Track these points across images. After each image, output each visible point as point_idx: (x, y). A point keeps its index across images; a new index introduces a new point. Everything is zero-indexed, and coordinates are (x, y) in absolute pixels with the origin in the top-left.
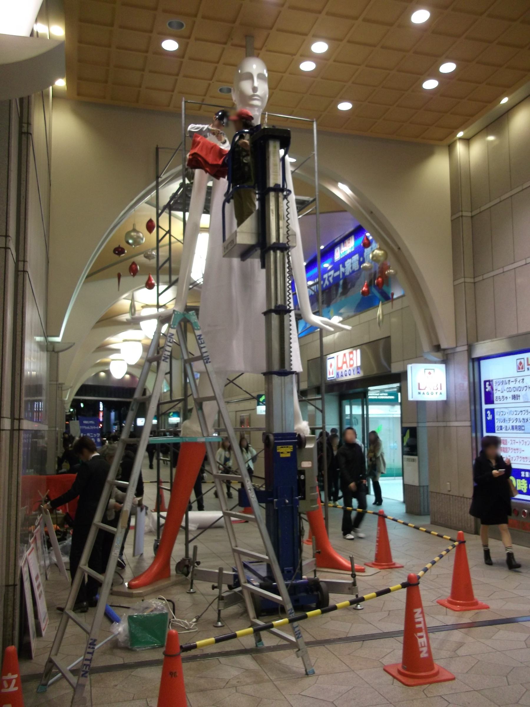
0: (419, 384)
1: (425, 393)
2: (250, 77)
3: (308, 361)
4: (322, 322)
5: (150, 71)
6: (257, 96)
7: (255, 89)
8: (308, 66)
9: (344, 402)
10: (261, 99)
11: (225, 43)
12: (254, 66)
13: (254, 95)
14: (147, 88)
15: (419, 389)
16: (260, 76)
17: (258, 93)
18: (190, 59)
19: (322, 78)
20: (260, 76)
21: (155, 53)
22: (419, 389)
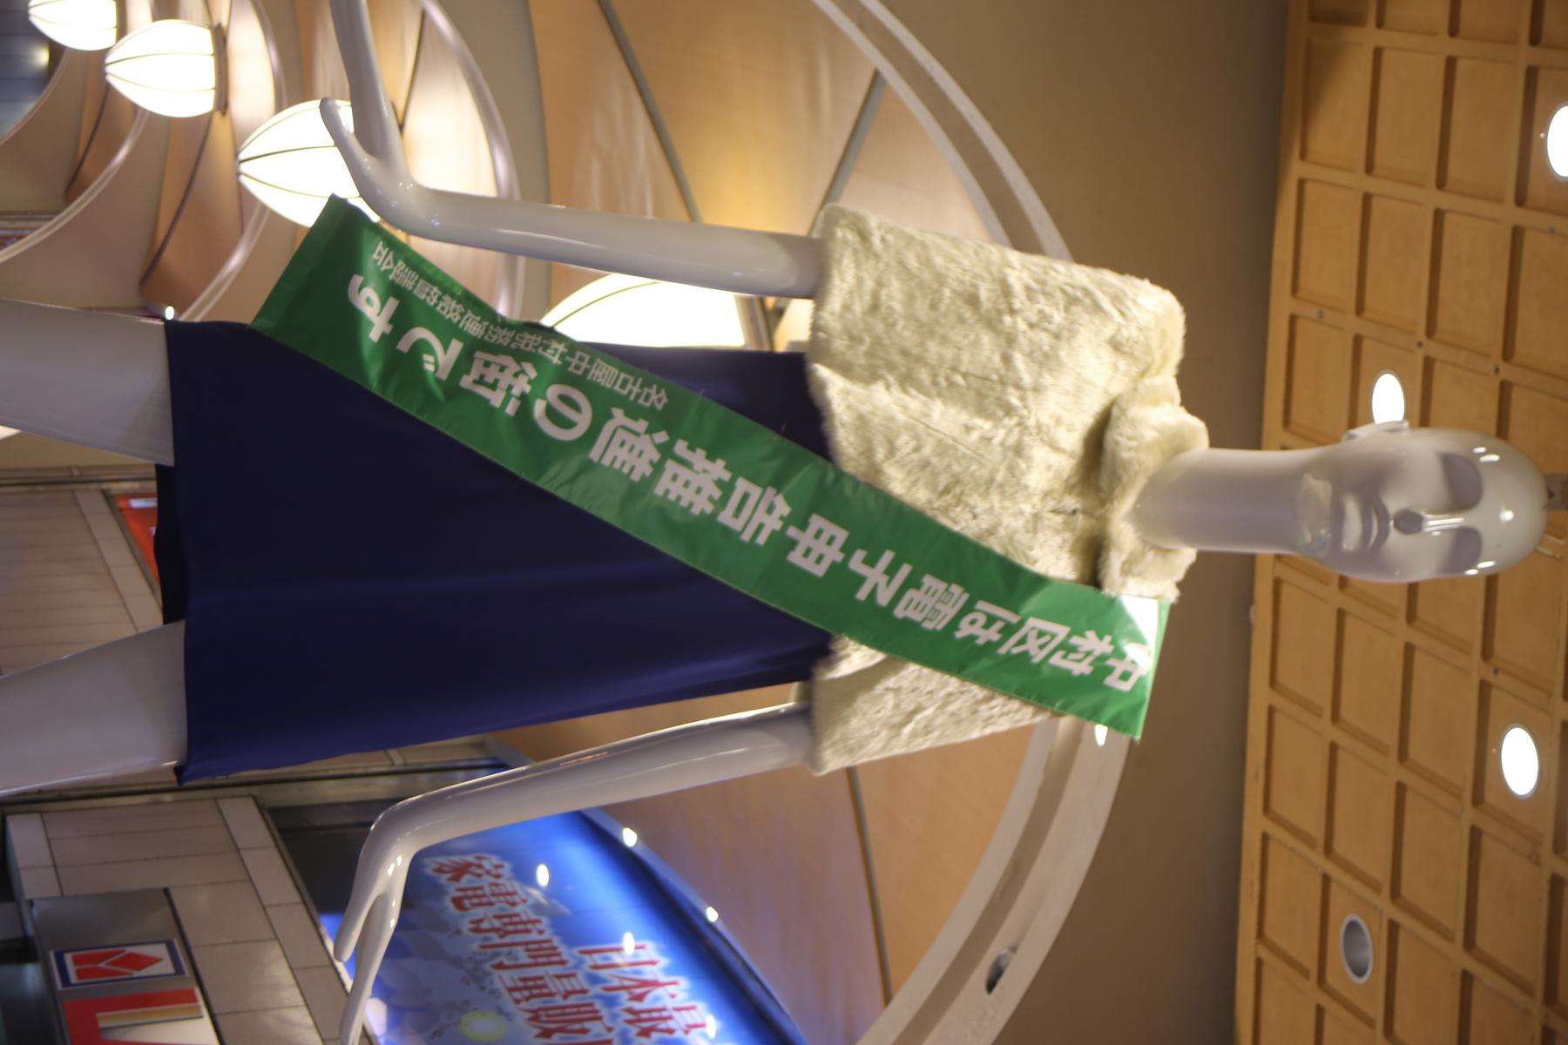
3: (166, 891)
4: (383, 900)
5: (1451, 64)
6: (1383, 533)
7: (1410, 522)
10: (1371, 553)
12: (1508, 515)
13: (1383, 516)
14: (1378, 53)
17: (1394, 536)
18: (1517, 234)
20: (1465, 544)
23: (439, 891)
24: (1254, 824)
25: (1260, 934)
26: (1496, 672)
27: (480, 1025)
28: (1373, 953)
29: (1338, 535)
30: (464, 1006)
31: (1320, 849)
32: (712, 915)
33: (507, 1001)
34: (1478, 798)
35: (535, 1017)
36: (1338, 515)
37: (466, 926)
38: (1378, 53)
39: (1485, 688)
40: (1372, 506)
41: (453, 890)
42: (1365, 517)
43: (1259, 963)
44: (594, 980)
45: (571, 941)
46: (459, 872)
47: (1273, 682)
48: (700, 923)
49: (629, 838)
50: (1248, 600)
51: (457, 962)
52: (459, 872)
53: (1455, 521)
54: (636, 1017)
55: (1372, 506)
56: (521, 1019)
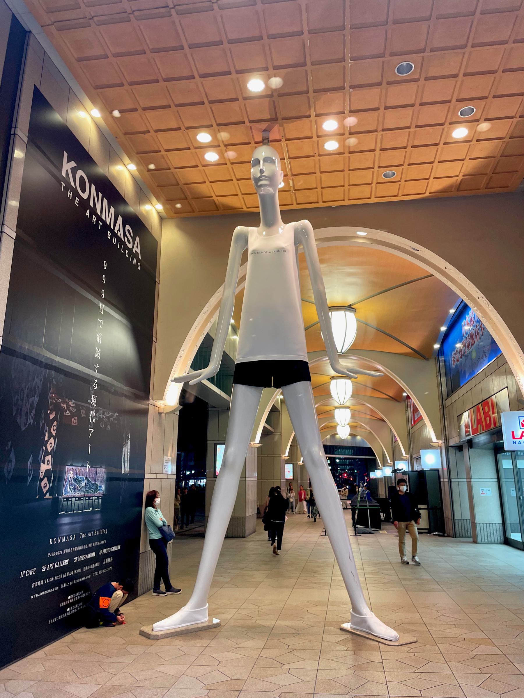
0: (513, 433)
1: (522, 442)
2: (257, 162)
6: (264, 176)
7: (262, 171)
8: (331, 146)
9: (500, 456)
11: (249, 143)
12: (263, 154)
13: (261, 177)
14: (217, 196)
15: (514, 438)
16: (266, 160)
18: (232, 163)
21: (204, 166)
22: (514, 438)
23: (457, 364)
24: (373, 200)
27: (474, 355)
28: (389, 171)
29: (266, 185)
30: (471, 359)
32: (452, 311)
33: (471, 350)
35: (472, 344)
36: (261, 186)
37: (461, 359)
38: (217, 196)
39: (320, 155)
41: (456, 362)
42: (261, 180)
44: (467, 333)
45: (462, 339)
46: (454, 361)
47: (343, 200)
48: (457, 313)
49: (443, 329)
50: (331, 207)
51: (466, 360)
52: (454, 361)
53: (261, 162)
54: (472, 325)
56: (473, 347)
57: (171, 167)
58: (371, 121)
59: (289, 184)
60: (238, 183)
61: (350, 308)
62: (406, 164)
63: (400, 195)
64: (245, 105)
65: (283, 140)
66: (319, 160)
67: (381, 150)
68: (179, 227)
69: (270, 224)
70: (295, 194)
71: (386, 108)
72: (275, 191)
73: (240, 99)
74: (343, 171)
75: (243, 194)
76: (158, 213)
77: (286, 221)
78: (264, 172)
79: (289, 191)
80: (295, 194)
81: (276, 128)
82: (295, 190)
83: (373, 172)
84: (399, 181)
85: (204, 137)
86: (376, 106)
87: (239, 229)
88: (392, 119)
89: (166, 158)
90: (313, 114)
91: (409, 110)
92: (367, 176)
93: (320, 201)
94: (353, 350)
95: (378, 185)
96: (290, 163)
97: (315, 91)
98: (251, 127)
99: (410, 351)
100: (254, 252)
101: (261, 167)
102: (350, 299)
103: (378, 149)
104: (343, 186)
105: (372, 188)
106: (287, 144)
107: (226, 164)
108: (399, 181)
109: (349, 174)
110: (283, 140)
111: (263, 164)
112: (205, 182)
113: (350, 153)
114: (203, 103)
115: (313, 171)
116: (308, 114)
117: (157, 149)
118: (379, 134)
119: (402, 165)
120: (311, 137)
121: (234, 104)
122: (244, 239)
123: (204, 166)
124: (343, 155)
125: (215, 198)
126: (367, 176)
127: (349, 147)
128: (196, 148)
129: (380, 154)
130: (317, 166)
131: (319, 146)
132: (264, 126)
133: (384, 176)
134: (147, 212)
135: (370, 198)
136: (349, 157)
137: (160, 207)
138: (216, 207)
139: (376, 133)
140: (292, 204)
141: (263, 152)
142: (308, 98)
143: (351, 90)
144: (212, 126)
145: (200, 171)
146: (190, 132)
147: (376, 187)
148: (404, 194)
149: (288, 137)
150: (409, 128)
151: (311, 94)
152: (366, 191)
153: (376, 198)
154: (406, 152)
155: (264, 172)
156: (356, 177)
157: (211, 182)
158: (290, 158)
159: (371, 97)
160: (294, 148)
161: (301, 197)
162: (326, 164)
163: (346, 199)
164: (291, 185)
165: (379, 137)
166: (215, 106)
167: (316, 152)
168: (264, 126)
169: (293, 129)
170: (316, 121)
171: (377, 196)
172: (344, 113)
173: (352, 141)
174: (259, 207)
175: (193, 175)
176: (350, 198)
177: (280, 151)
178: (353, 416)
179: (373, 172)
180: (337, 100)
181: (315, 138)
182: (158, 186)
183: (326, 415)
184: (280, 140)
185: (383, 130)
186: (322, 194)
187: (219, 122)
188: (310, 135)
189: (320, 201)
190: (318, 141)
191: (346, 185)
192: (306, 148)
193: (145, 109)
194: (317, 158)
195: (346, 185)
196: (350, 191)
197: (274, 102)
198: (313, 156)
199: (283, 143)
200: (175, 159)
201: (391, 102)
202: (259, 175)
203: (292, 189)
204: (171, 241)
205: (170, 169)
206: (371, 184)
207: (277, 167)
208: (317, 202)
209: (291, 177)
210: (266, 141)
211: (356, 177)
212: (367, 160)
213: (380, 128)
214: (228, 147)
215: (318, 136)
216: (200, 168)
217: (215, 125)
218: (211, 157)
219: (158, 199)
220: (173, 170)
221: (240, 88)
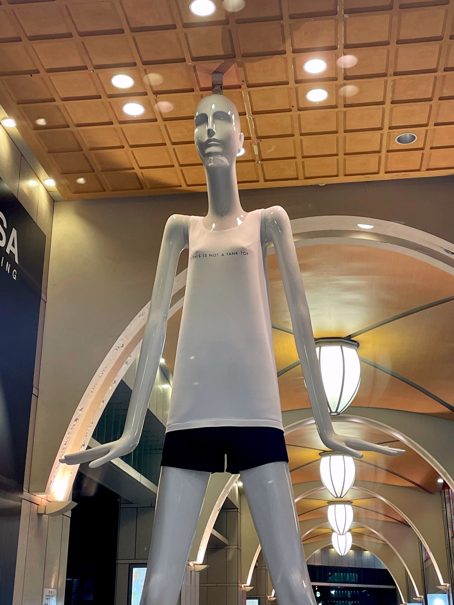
2: (203, 119)
6: (215, 140)
7: (211, 133)
8: (317, 96)
11: (192, 90)
12: (213, 106)
13: (209, 141)
14: (141, 168)
16: (217, 116)
18: (165, 120)
19: (345, 107)
21: (121, 123)
24: (383, 176)
25: (419, 170)
26: (293, 106)
28: (406, 134)
29: (217, 153)
31: (380, 154)
34: (335, 107)
36: (210, 154)
38: (141, 168)
39: (299, 109)
40: (206, 145)
43: (428, 170)
47: (337, 176)
50: (317, 186)
53: (210, 119)
55: (206, 145)
57: (70, 124)
58: (378, 60)
59: (252, 150)
60: (174, 149)
61: (349, 340)
62: (432, 123)
63: (424, 168)
64: (186, 35)
65: (244, 86)
66: (299, 116)
67: (393, 102)
68: (81, 214)
69: (223, 211)
70: (262, 165)
71: (399, 42)
72: (231, 162)
73: (179, 25)
74: (336, 132)
75: (181, 165)
76: (48, 192)
77: (248, 208)
78: (214, 133)
79: (254, 161)
80: (262, 165)
81: (233, 68)
82: (262, 160)
83: (382, 135)
84: (422, 149)
85: (122, 81)
86: (385, 39)
87: (174, 218)
88: (408, 58)
89: (62, 110)
90: (289, 49)
91: (435, 46)
92: (372, 141)
93: (301, 177)
94: (355, 409)
95: (389, 154)
96: (254, 120)
97: (292, 17)
98: (194, 67)
99: (447, 410)
100: (198, 255)
101: (210, 127)
102: (350, 328)
103: (388, 101)
104: (337, 155)
105: (380, 158)
106: (249, 93)
107: (156, 120)
108: (422, 149)
109: (345, 137)
110: (244, 86)
111: (213, 122)
112: (123, 147)
113: (345, 106)
114: (121, 31)
115: (290, 133)
116: (281, 49)
117: (49, 97)
118: (390, 79)
119: (426, 125)
120: (287, 83)
121: (169, 35)
122: (183, 234)
123: (121, 123)
124: (336, 110)
125: (137, 170)
126: (372, 141)
127: (345, 98)
128: (110, 96)
129: (391, 110)
130: (296, 125)
131: (299, 95)
132: (215, 65)
133: (399, 140)
134: (31, 191)
135: (377, 173)
136: (345, 113)
137: (51, 183)
138: (140, 183)
139: (385, 78)
140: (258, 181)
141: (212, 104)
142: (282, 26)
143: (346, 16)
144: (135, 64)
145: (115, 129)
146: (101, 72)
147: (387, 157)
148: (430, 167)
149: (252, 81)
150: (435, 71)
151: (286, 21)
152: (371, 162)
153: (386, 173)
154: (431, 106)
155: (214, 133)
156: (355, 143)
157: (132, 146)
158: (254, 113)
159: (377, 27)
160: (262, 98)
161: (272, 171)
162: (310, 122)
163: (341, 173)
164: (256, 153)
165: (390, 84)
166: (139, 36)
167: (294, 103)
168: (215, 65)
169: (258, 70)
170: (294, 59)
171: (389, 170)
172: (335, 48)
173: (350, 90)
174: (206, 185)
175: (103, 137)
176: (347, 173)
177: (238, 102)
178: (356, 518)
179: (382, 135)
180: (325, 31)
181: (292, 83)
182: (49, 152)
183: (313, 515)
184: (240, 87)
185: (395, 74)
186: (303, 167)
187: (145, 59)
188: (284, 79)
189: (301, 177)
190: (296, 89)
191: (341, 154)
192: (278, 98)
193: (33, 38)
194: (295, 113)
195: (341, 154)
196: (347, 162)
197: (230, 31)
198: (290, 110)
199: (244, 92)
200: (77, 113)
201: (406, 34)
202: (206, 138)
203: (257, 158)
204: (66, 234)
205: (69, 127)
206: (379, 152)
207: (235, 127)
208: (297, 179)
209: (256, 141)
210: (218, 88)
211: (355, 143)
212: (372, 116)
213: (391, 71)
214: (158, 96)
215: (297, 82)
216: (116, 125)
217: (139, 63)
218: (134, 109)
219: (49, 172)
220: (73, 129)
221: (179, 10)
